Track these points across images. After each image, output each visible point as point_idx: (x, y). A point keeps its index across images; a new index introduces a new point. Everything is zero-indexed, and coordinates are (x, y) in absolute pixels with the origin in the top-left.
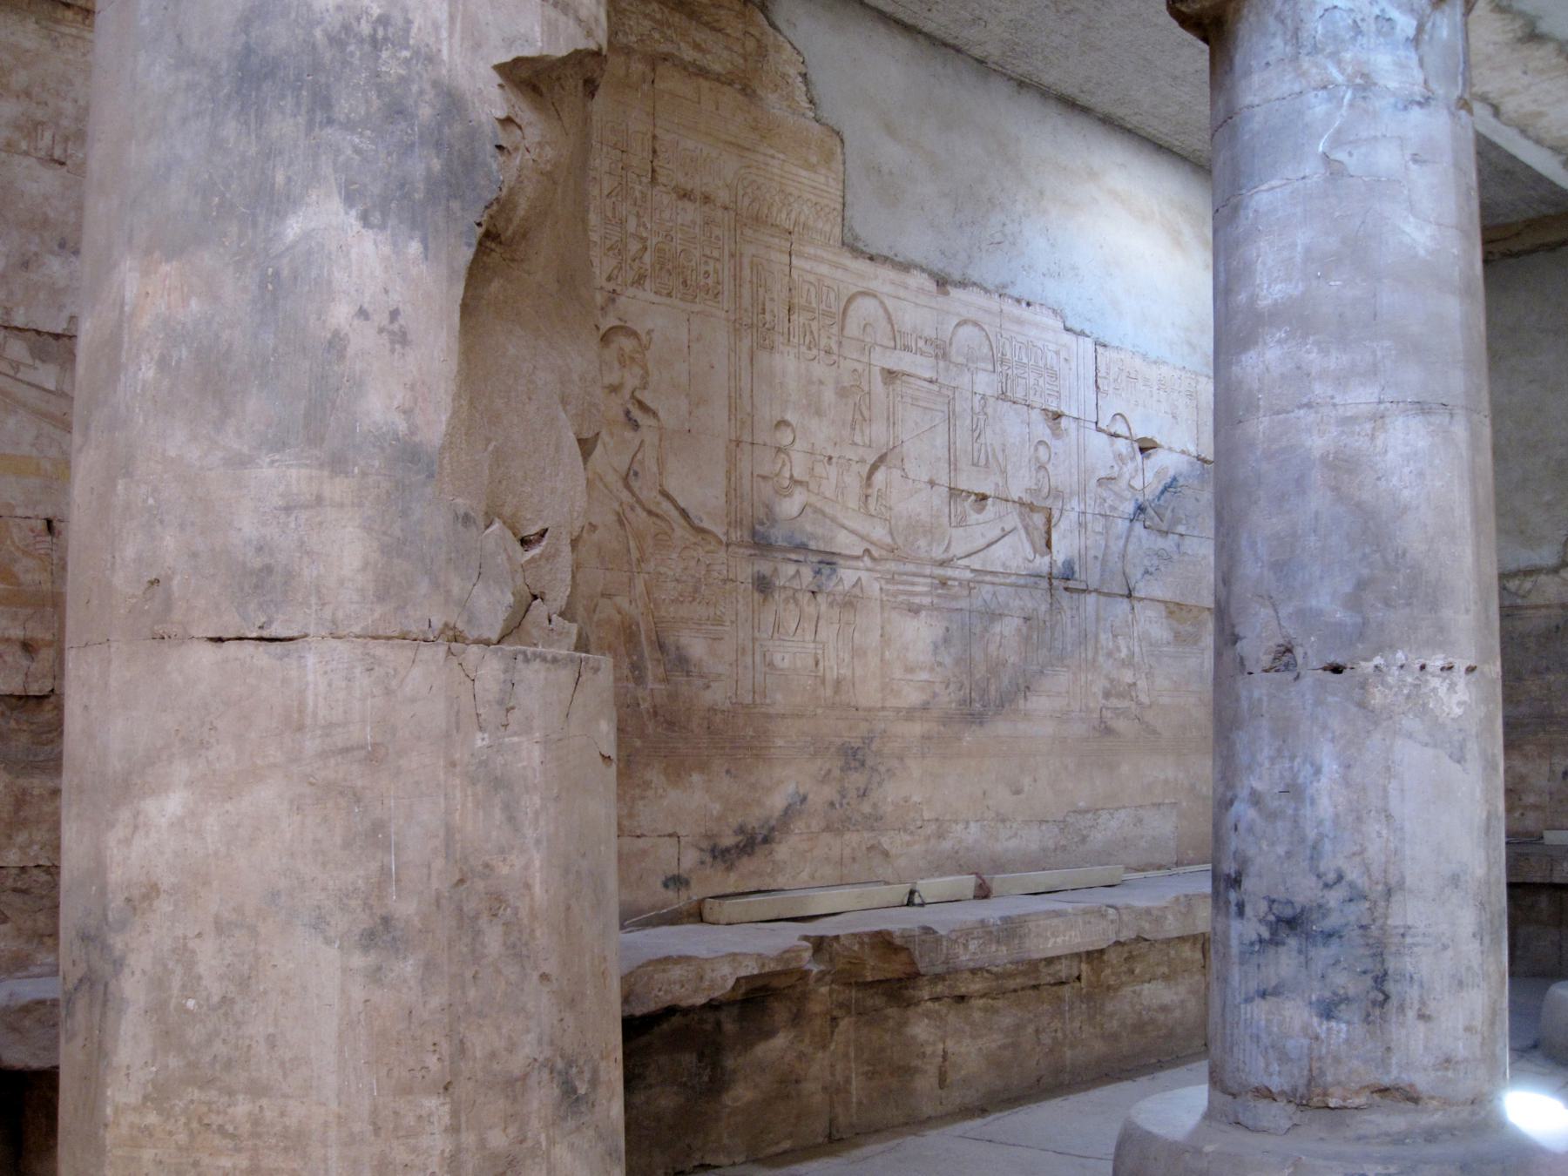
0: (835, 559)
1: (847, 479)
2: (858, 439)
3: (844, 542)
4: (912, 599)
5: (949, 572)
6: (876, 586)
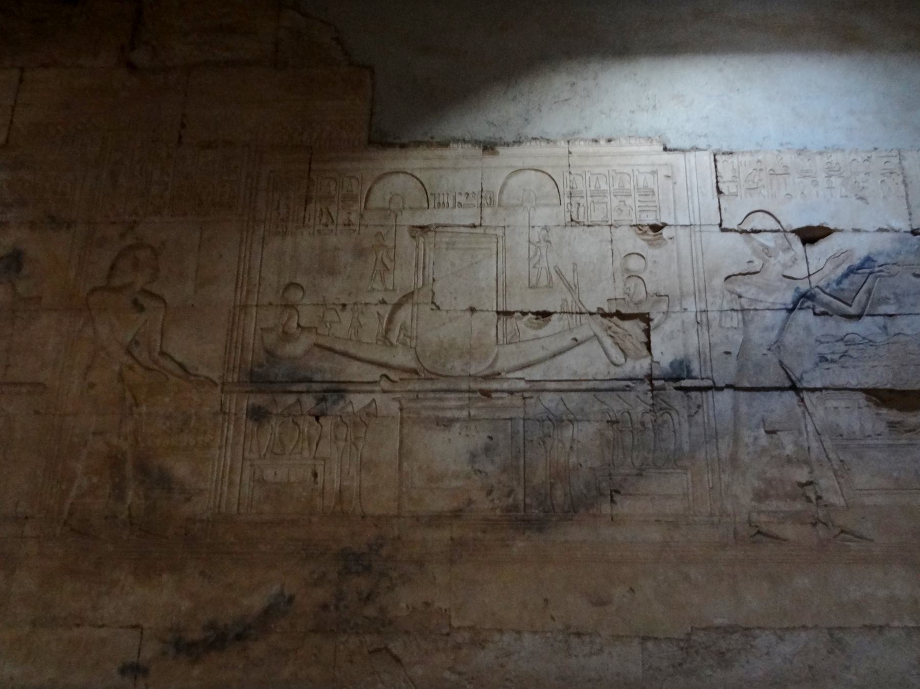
0: (343, 386)
1: (362, 320)
3: (354, 371)
4: (441, 414)
5: (494, 385)
6: (395, 406)
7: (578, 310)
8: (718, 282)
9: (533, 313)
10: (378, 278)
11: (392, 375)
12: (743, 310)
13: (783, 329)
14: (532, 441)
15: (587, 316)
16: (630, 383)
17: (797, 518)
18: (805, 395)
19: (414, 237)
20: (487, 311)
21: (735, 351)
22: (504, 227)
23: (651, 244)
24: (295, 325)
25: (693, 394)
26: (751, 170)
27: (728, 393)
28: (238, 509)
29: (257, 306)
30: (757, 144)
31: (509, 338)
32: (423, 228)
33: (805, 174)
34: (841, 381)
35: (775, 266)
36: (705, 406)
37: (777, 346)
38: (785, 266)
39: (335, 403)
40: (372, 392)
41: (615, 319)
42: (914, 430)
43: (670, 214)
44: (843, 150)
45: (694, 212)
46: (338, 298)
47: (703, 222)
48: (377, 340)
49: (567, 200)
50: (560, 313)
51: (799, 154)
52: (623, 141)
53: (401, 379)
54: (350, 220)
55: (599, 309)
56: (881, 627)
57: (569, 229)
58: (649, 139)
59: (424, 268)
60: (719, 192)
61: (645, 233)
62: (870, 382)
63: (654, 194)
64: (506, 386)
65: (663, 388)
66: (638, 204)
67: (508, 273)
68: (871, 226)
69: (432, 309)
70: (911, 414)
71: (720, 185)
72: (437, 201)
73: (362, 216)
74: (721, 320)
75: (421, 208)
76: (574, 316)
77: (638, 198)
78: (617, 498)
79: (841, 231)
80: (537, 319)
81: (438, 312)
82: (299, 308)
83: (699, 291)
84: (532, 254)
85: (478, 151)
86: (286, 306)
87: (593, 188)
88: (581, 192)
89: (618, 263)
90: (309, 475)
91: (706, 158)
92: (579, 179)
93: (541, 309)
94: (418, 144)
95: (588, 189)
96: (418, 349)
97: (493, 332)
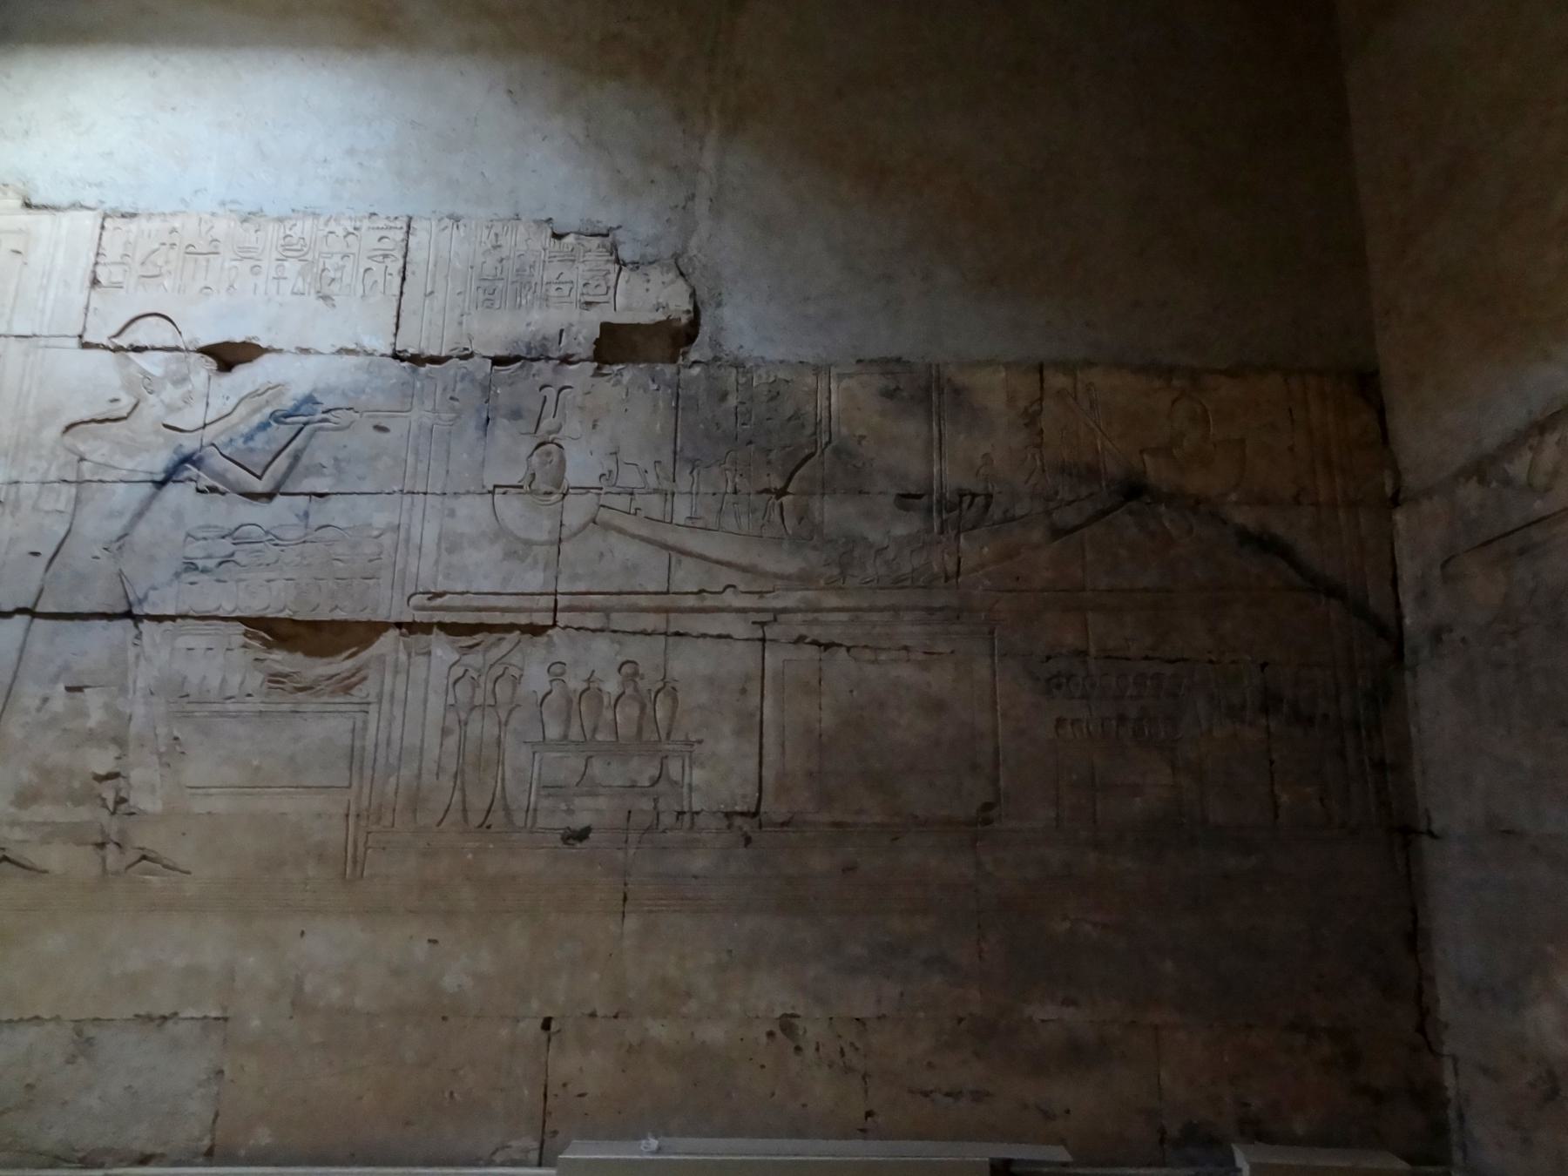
8: (52, 432)
13: (139, 515)
17: (73, 834)
18: (146, 626)
30: (183, 200)
33: (244, 254)
34: (208, 606)
35: (153, 409)
38: (171, 409)
42: (311, 688)
44: (315, 215)
56: (164, 1018)
62: (255, 606)
68: (326, 345)
70: (325, 660)
79: (280, 351)
91: (87, 222)
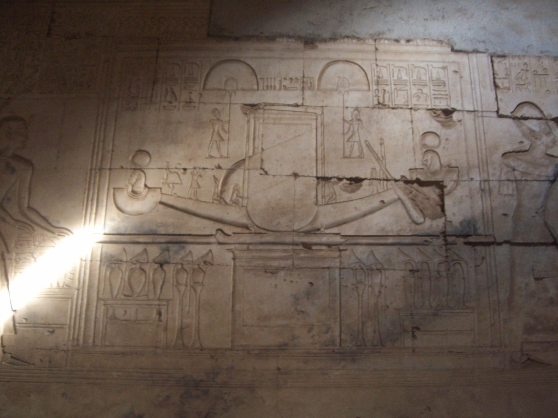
2: (214, 153)
4: (269, 263)
6: (230, 255)
7: (385, 178)
8: (497, 157)
9: (347, 179)
10: (215, 146)
11: (228, 229)
12: (516, 181)
13: (547, 197)
14: (346, 286)
15: (393, 182)
16: (428, 238)
19: (246, 114)
20: (309, 176)
21: (511, 213)
22: (322, 107)
23: (444, 125)
24: (142, 185)
25: (479, 248)
26: (519, 71)
27: (505, 247)
28: (94, 342)
29: (110, 169)
30: (523, 50)
31: (327, 199)
32: (254, 106)
36: (488, 258)
37: (543, 209)
39: (177, 252)
40: (209, 243)
41: (415, 185)
43: (458, 101)
45: (477, 101)
46: (180, 164)
47: (484, 109)
48: (214, 199)
49: (375, 87)
50: (370, 179)
51: (555, 60)
52: (420, 42)
53: (234, 233)
54: (191, 99)
55: (402, 177)
57: (376, 110)
58: (440, 42)
59: (254, 139)
60: (496, 86)
61: (438, 116)
63: (445, 85)
64: (324, 239)
65: (454, 244)
66: (433, 92)
67: (326, 144)
69: (261, 174)
71: (497, 81)
72: (265, 84)
73: (201, 95)
74: (500, 187)
75: (252, 90)
76: (382, 182)
77: (432, 88)
78: (417, 333)
80: (350, 184)
81: (266, 176)
82: (146, 171)
83: (483, 163)
84: (346, 130)
85: (301, 46)
86: (135, 169)
87: (396, 78)
88: (386, 80)
89: (418, 138)
90: (154, 315)
92: (384, 71)
93: (354, 175)
94: (249, 38)
95: (392, 79)
96: (249, 208)
97: (314, 194)
